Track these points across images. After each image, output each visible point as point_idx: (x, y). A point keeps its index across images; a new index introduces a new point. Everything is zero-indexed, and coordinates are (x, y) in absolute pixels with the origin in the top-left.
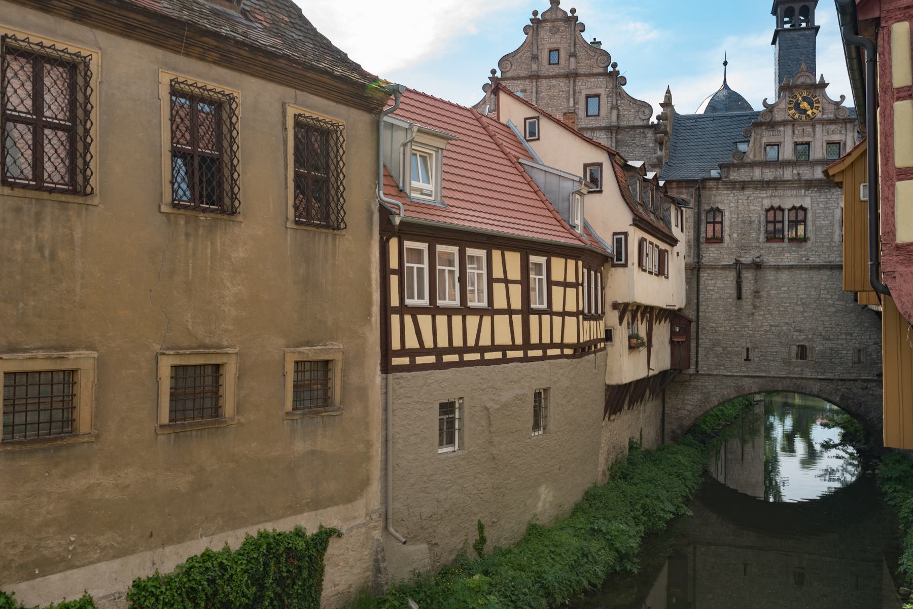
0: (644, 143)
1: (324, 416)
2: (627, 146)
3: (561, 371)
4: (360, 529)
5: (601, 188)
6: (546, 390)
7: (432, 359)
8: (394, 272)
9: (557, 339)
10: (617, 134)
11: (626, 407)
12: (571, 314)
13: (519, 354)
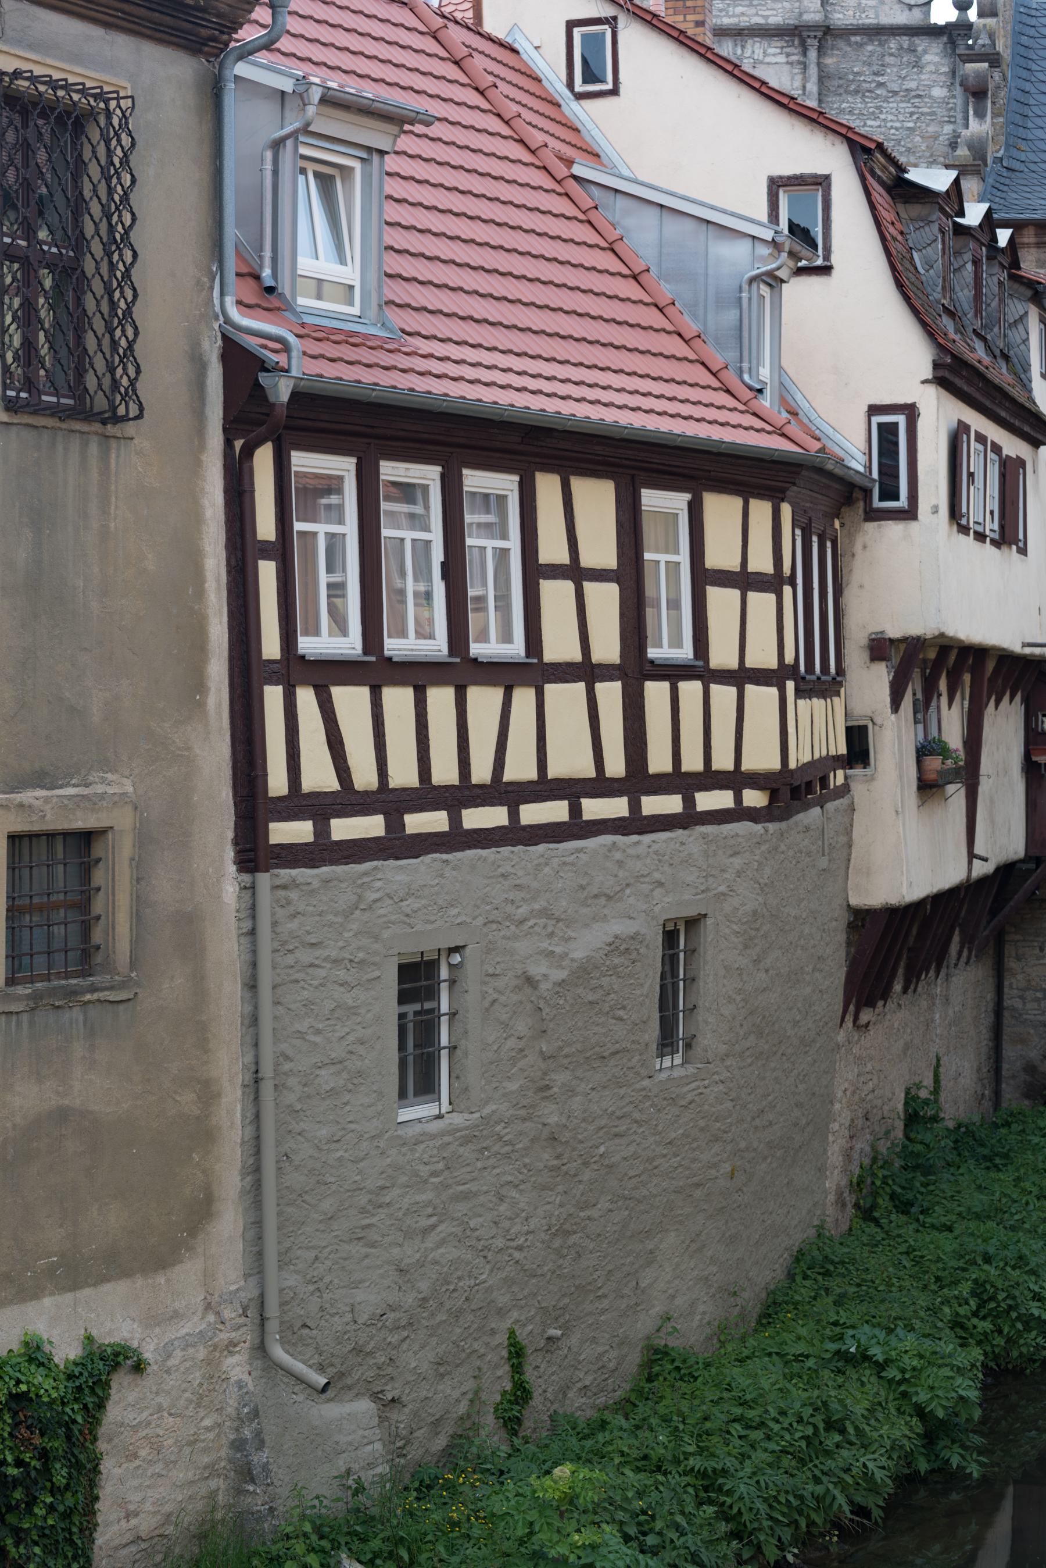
0: (913, 85)
1: (89, 1002)
2: (857, 92)
3: (737, 862)
4: (191, 1350)
5: (827, 257)
6: (693, 923)
7: (372, 826)
8: (265, 550)
9: (723, 761)
10: (821, 51)
11: (898, 987)
12: (761, 677)
13: (617, 807)
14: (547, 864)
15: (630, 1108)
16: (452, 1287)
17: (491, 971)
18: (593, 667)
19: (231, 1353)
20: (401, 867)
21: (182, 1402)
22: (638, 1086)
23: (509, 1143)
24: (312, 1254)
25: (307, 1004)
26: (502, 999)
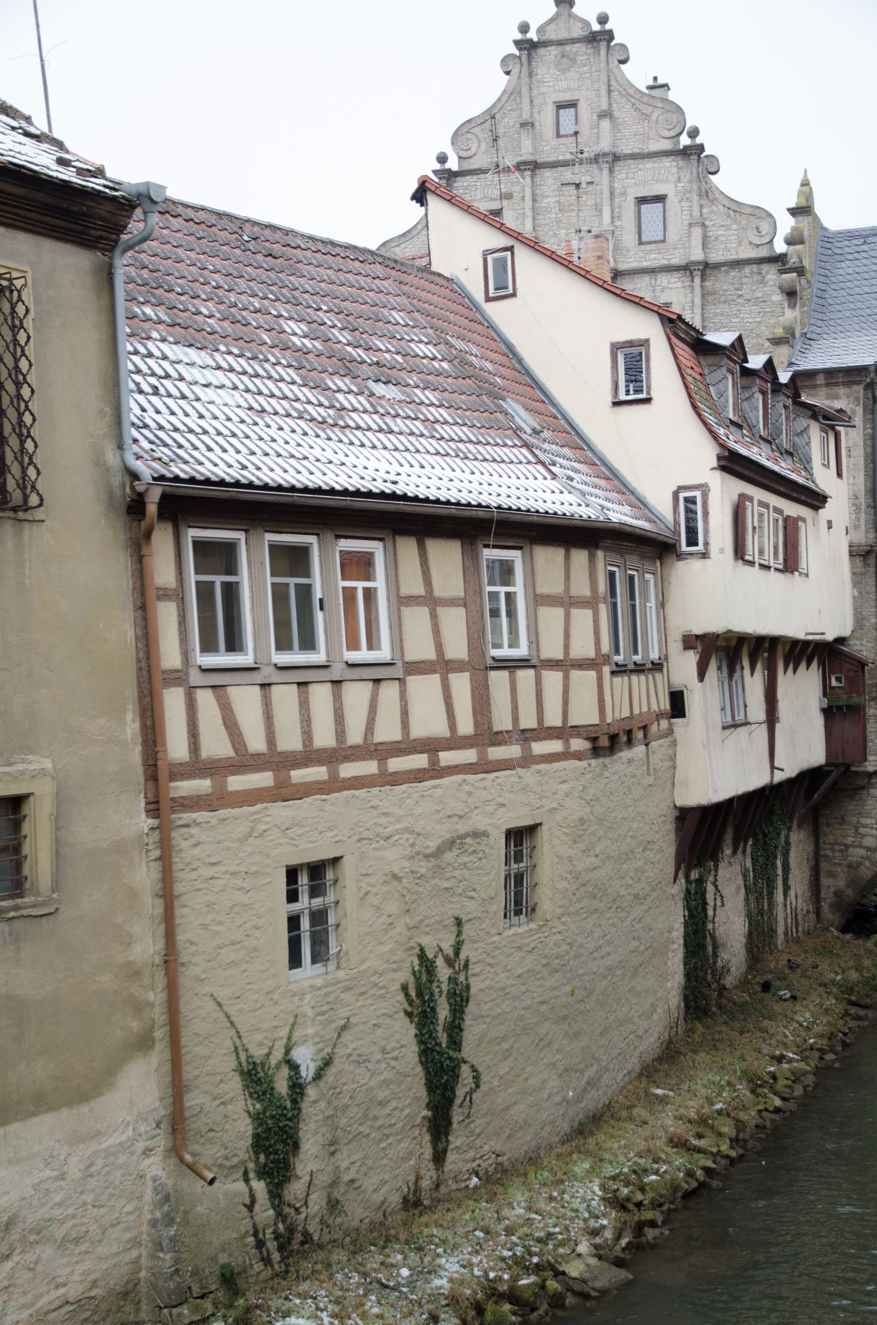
0: (760, 295)
1: (13, 918)
2: (725, 302)
3: (565, 787)
4: (111, 1159)
5: (648, 393)
6: (532, 829)
7: (264, 779)
8: (164, 595)
10: (703, 280)
11: (728, 851)
12: (582, 665)
13: (469, 756)
14: (408, 797)
15: (484, 955)
16: (337, 1091)
17: (364, 872)
18: (448, 662)
19: (148, 1156)
20: (287, 806)
21: (105, 1196)
22: (489, 941)
23: (384, 987)
24: (218, 1078)
25: (210, 905)
26: (374, 890)
